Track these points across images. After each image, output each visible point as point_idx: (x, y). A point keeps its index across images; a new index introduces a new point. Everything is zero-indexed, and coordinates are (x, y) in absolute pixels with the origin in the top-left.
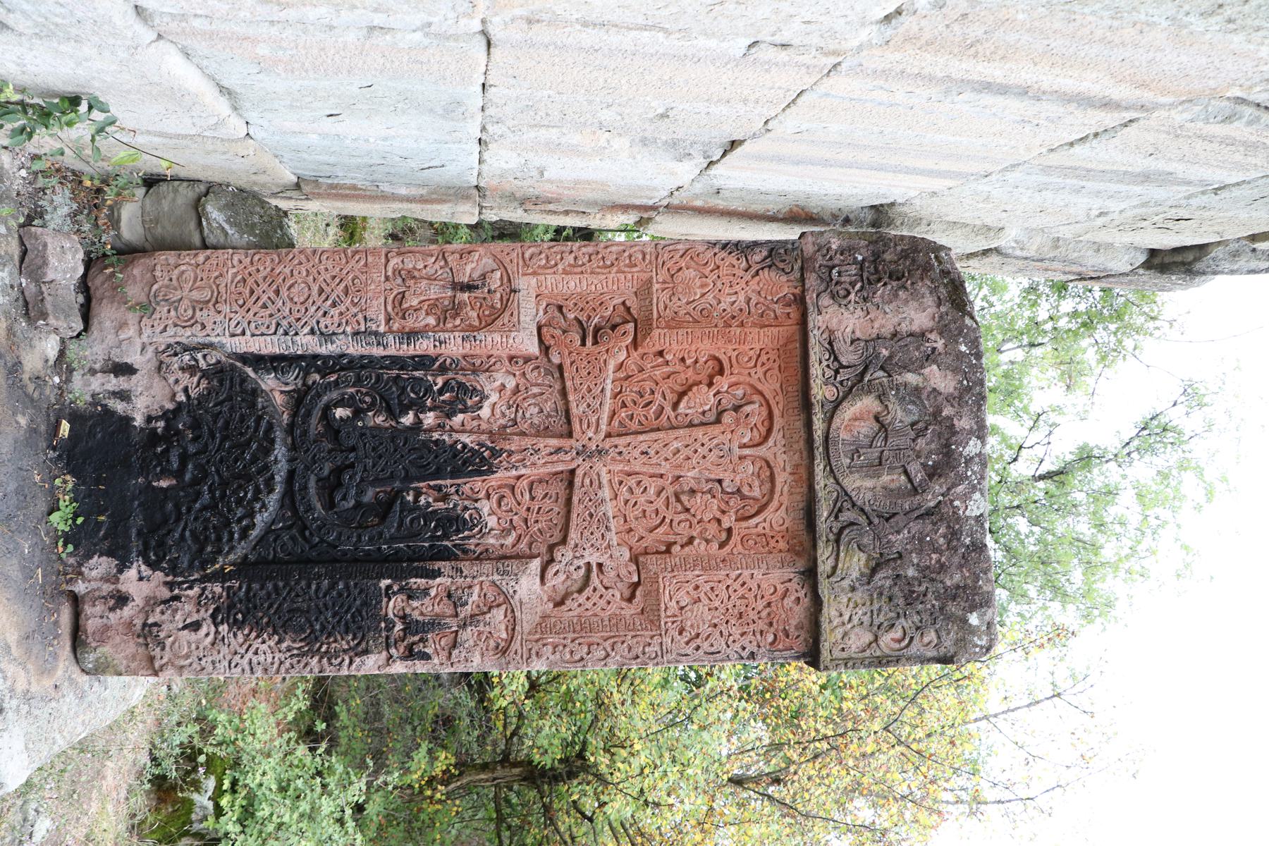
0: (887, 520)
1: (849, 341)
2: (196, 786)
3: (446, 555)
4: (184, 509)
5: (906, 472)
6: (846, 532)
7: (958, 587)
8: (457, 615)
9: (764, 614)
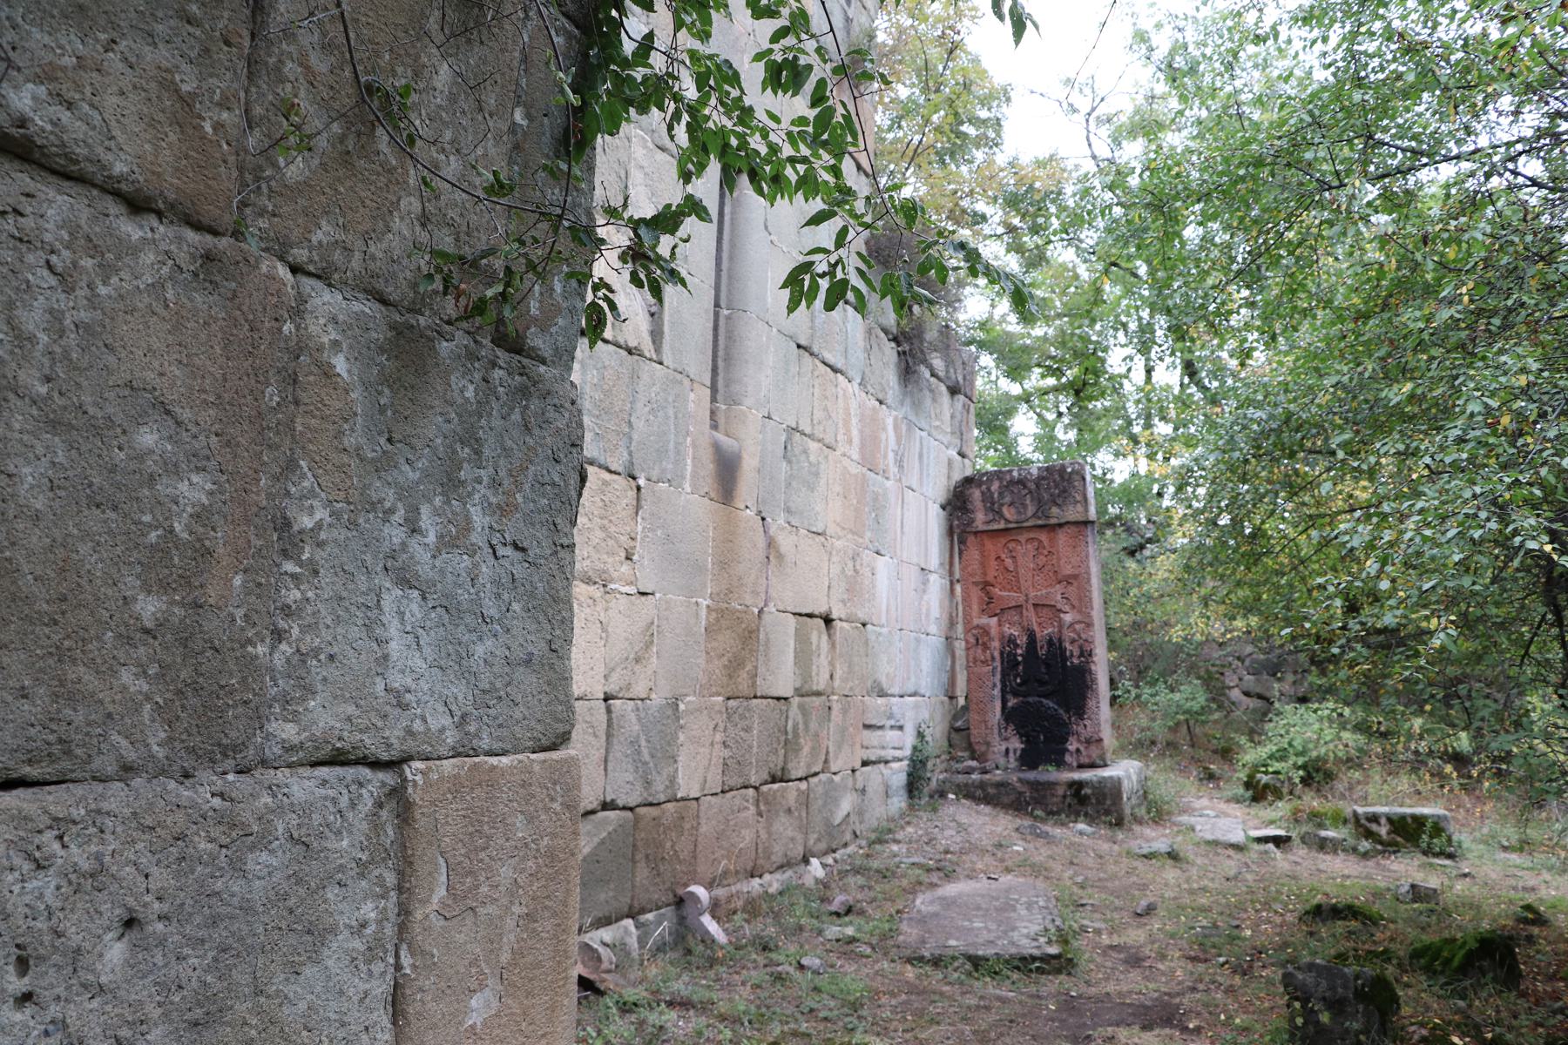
2: (1259, 781)
3: (1060, 644)
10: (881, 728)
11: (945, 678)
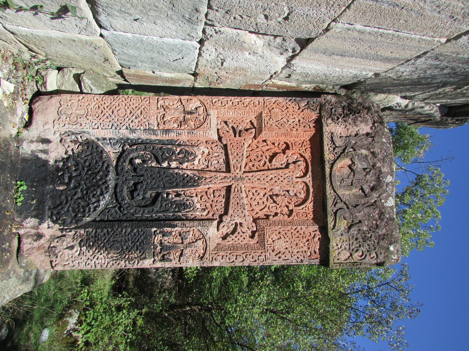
0: (355, 207)
1: (339, 137)
4: (69, 198)
5: (362, 189)
6: (339, 211)
7: (384, 235)
8: (182, 243)
9: (306, 244)
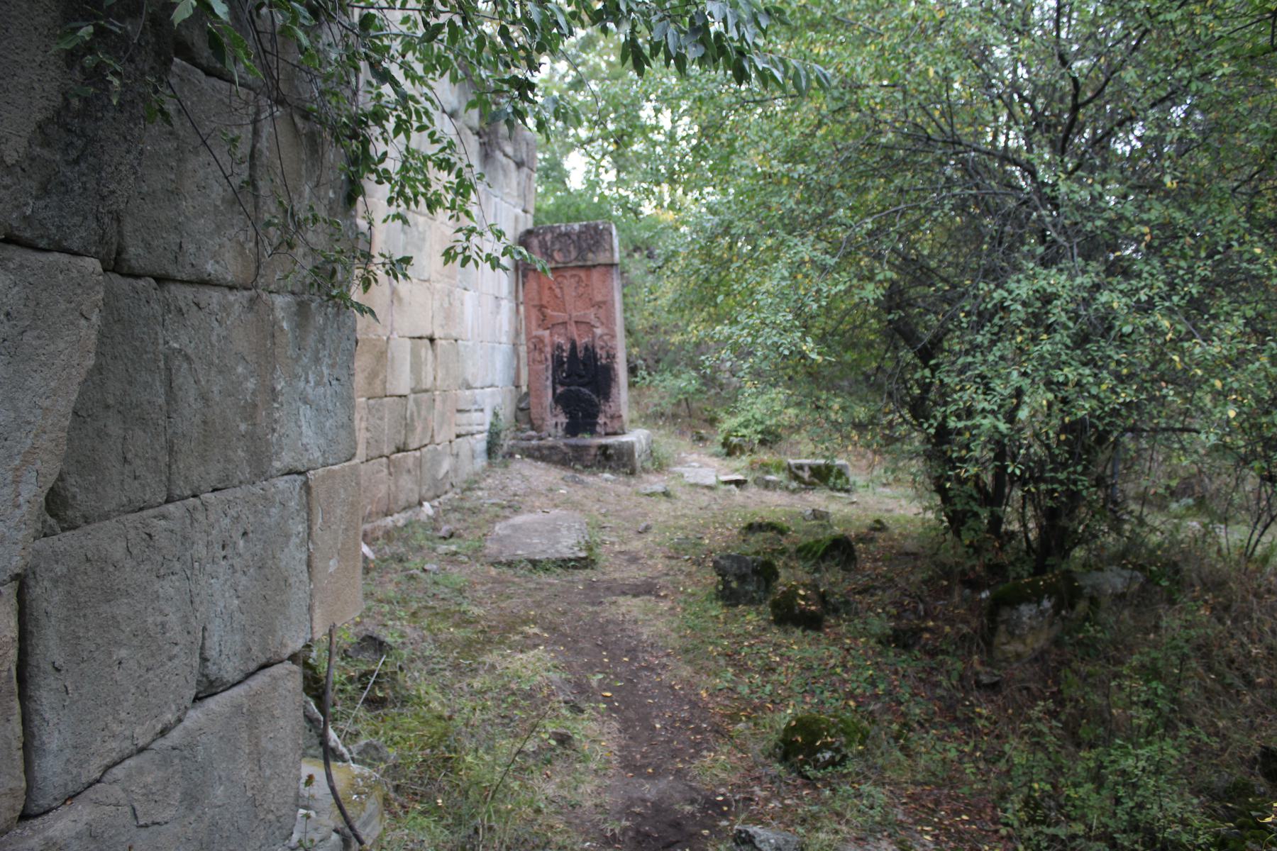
10: (469, 411)
11: (513, 373)
